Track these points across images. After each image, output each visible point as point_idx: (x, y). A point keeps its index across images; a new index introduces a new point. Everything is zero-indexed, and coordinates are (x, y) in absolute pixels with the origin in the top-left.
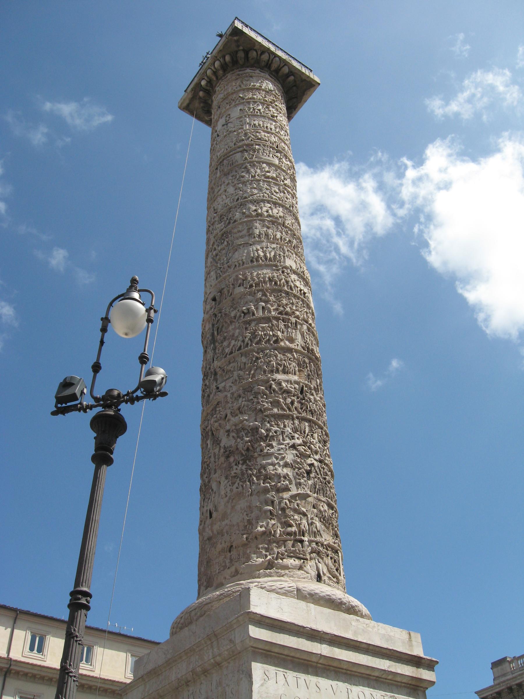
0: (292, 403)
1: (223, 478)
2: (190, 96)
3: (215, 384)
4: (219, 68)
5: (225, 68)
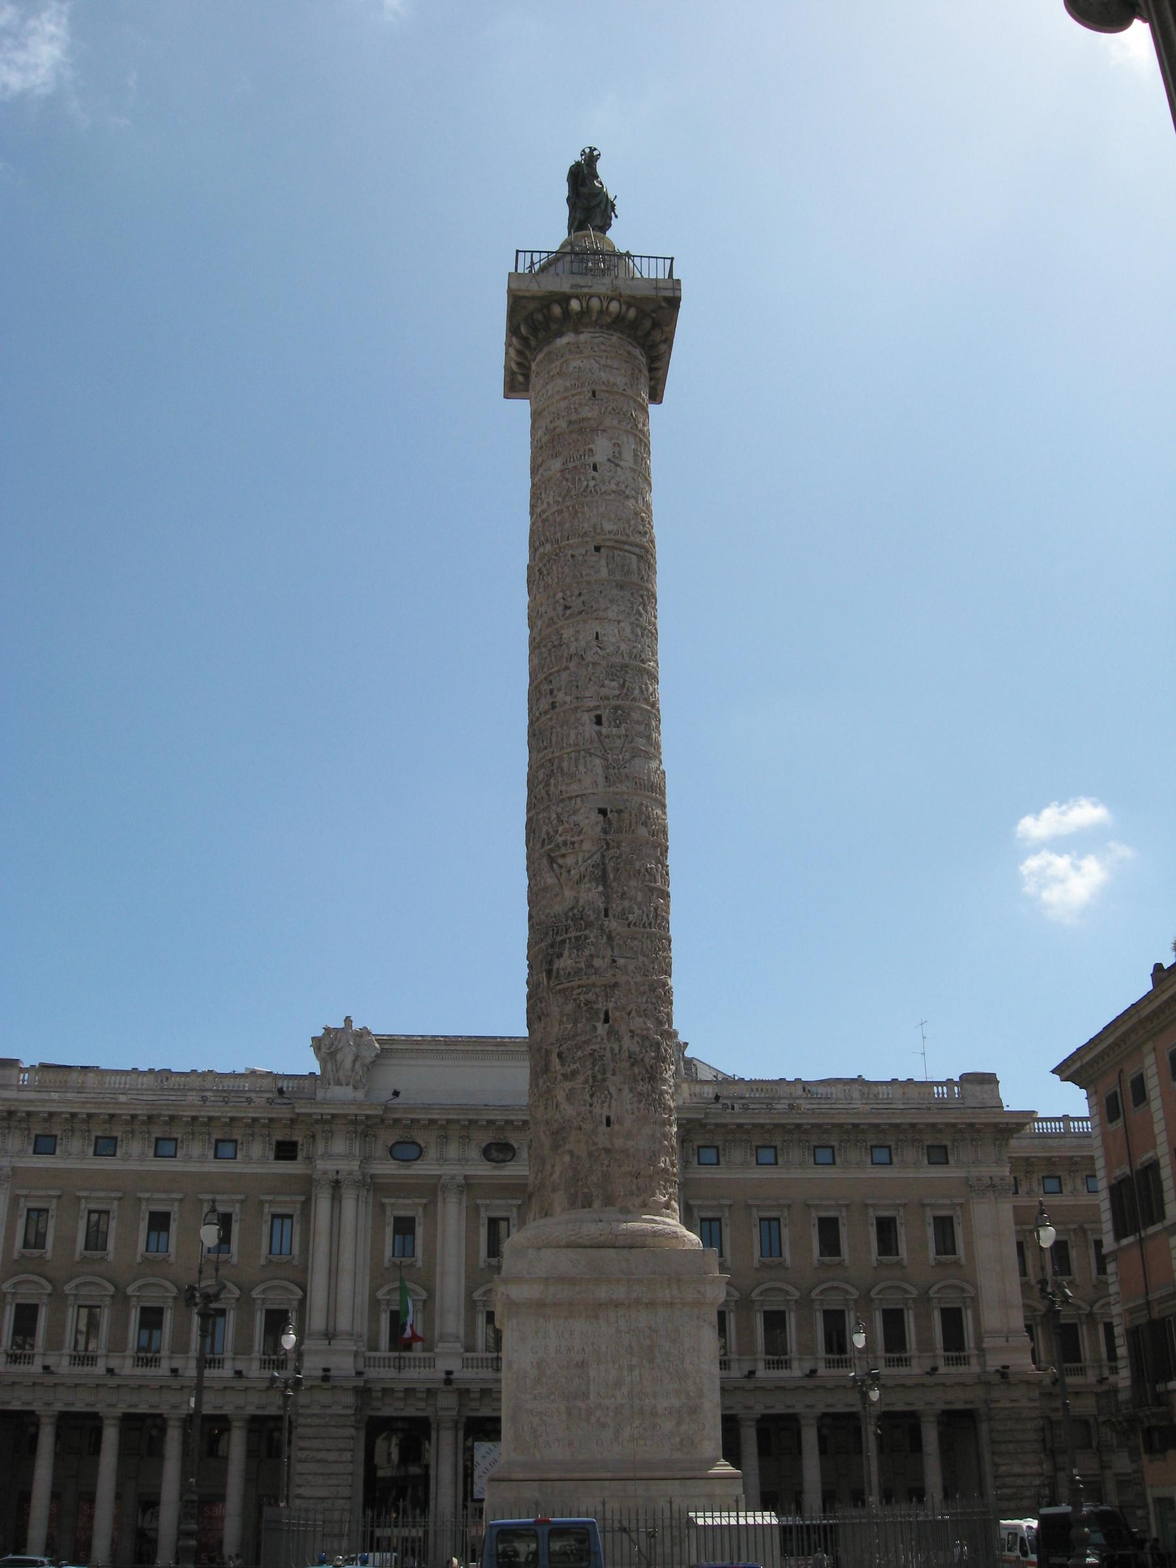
1: (626, 1089)
2: (539, 294)
3: (609, 952)
4: (614, 316)
5: (618, 323)
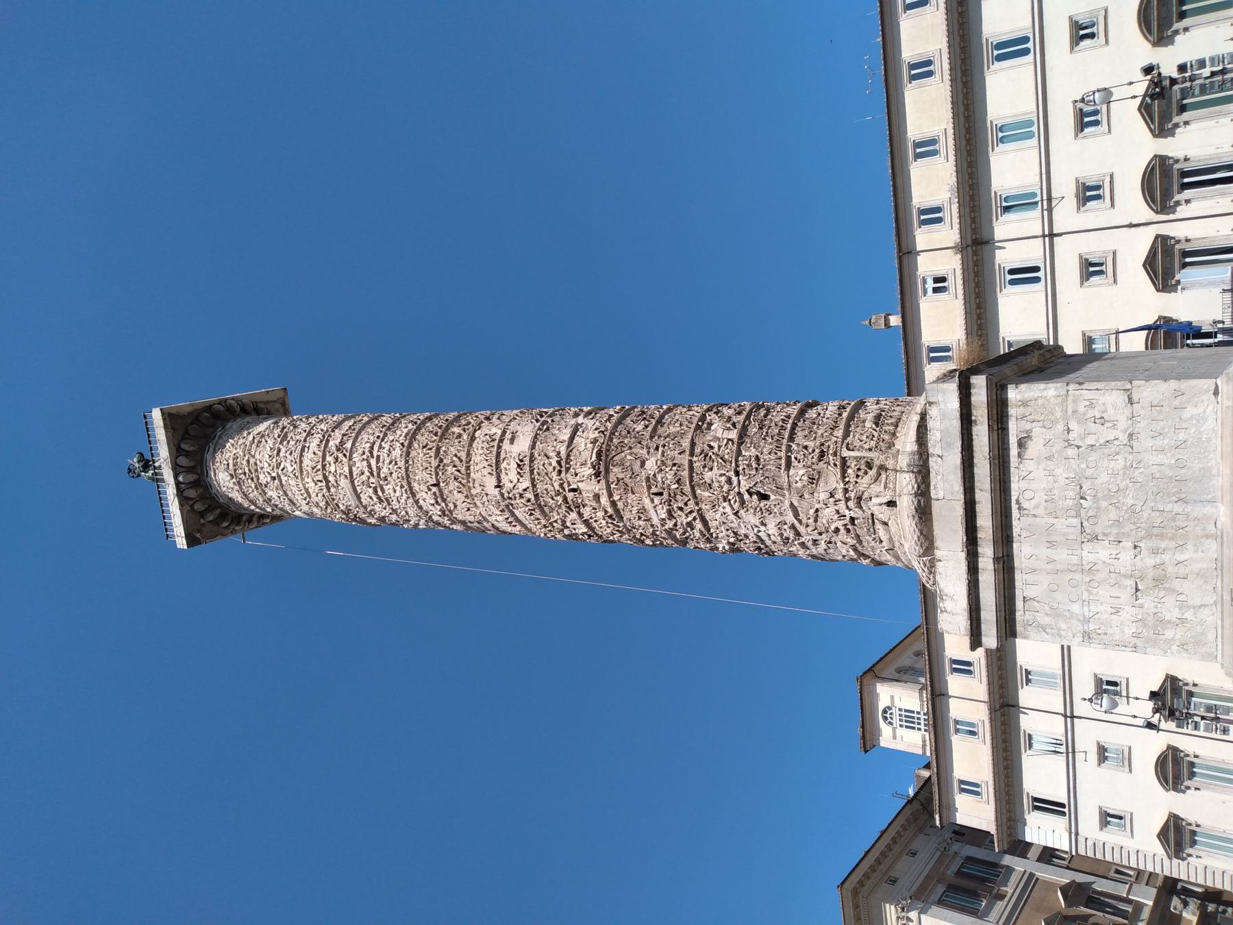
0: (681, 509)
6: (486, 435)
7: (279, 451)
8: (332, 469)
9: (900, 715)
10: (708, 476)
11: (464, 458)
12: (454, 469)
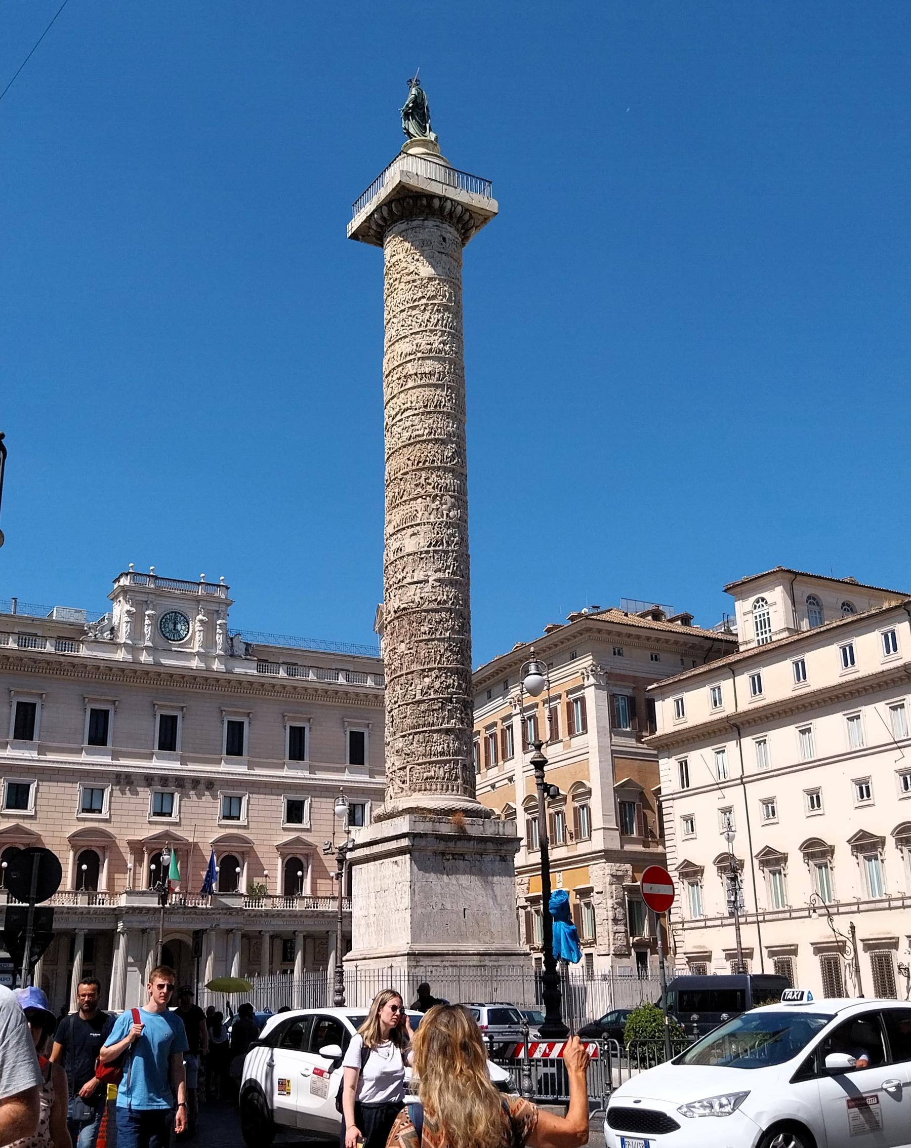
6: (416, 510)
7: (404, 311)
8: (394, 378)
9: (764, 614)
10: (398, 688)
11: (404, 499)
12: (397, 494)
